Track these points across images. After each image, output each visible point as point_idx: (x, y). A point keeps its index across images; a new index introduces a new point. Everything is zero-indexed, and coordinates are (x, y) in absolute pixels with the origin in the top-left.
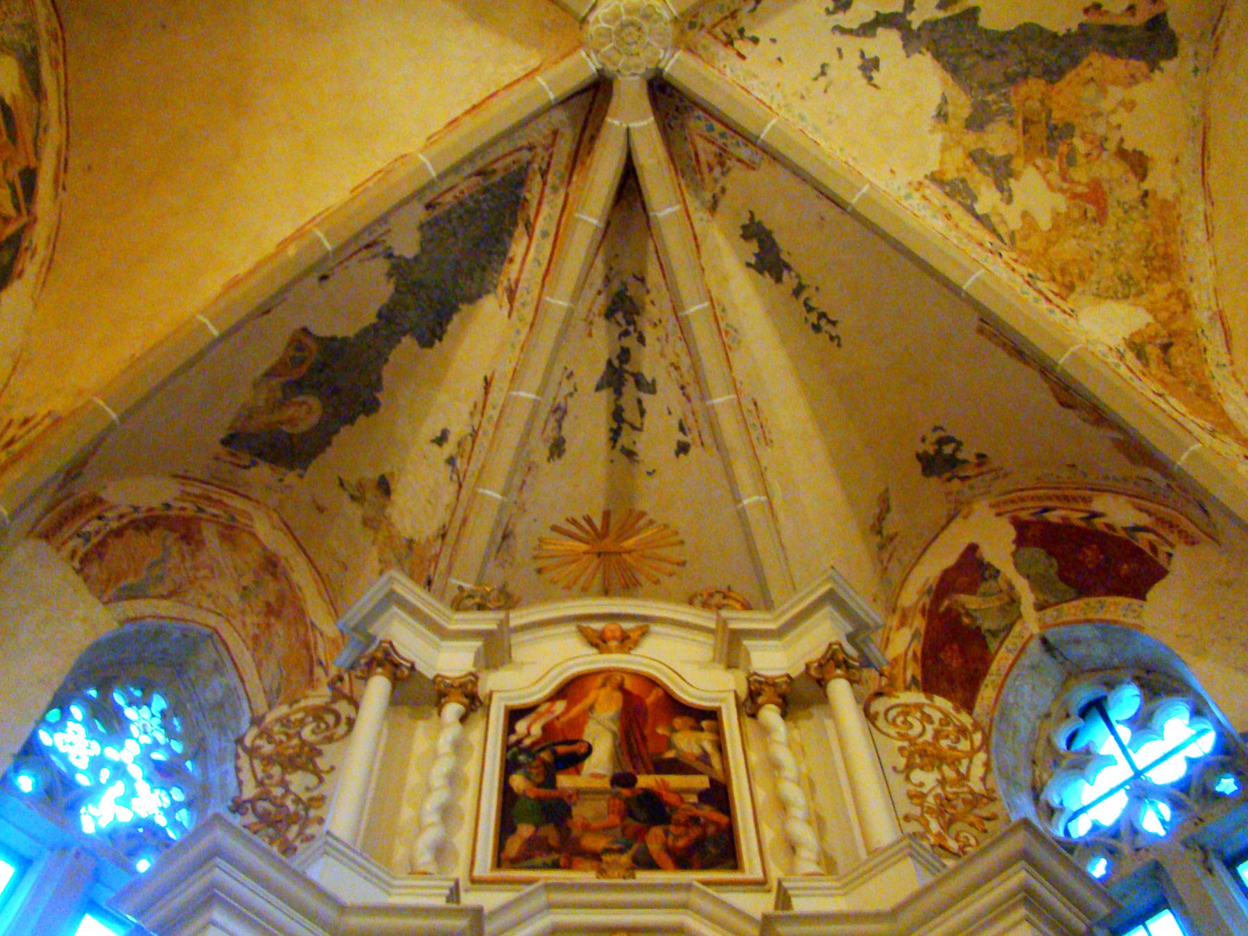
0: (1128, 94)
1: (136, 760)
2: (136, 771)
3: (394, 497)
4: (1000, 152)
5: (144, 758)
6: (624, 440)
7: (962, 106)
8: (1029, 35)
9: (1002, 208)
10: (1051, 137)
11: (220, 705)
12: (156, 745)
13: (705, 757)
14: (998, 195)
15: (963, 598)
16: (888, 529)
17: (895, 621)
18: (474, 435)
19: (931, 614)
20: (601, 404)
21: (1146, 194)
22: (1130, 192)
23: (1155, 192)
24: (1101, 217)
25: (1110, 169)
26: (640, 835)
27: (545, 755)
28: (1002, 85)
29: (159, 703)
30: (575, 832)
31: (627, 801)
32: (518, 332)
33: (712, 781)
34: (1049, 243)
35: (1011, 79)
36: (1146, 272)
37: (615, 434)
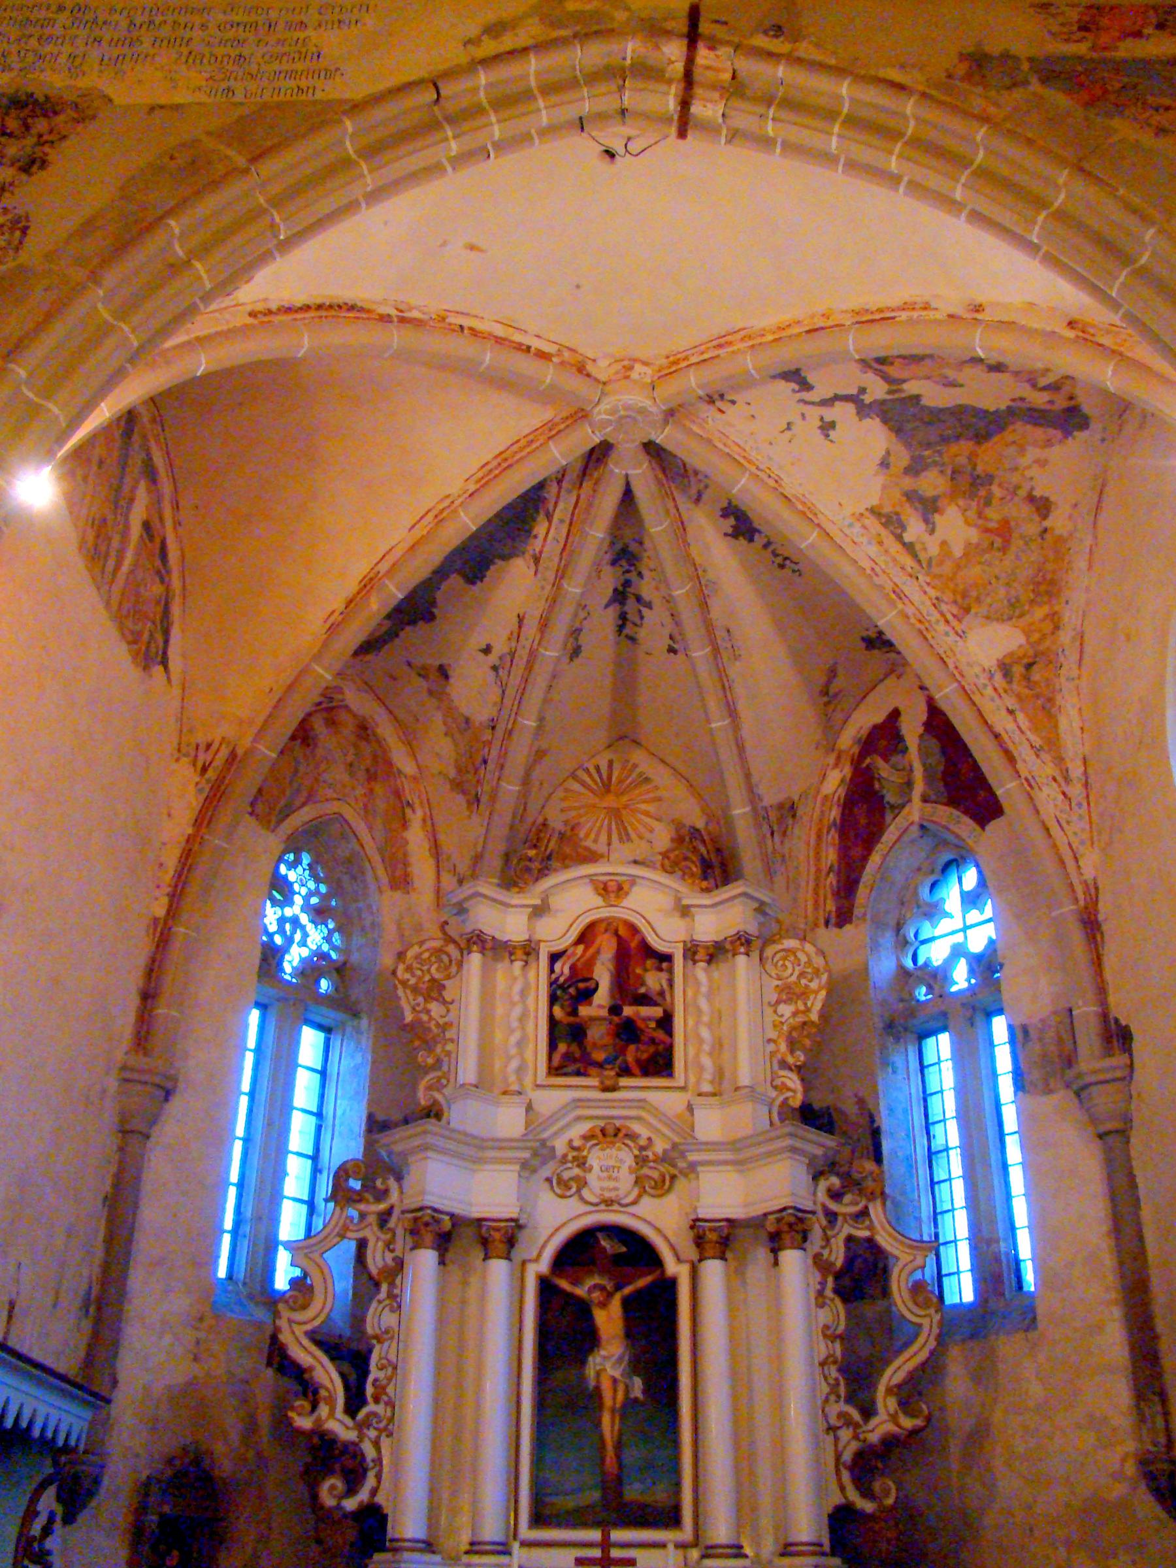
0: (1047, 453)
1: (302, 910)
2: (304, 919)
3: (452, 681)
4: (930, 493)
5: (306, 908)
6: (626, 631)
7: (902, 458)
8: (960, 412)
9: (926, 537)
10: (973, 485)
11: (349, 861)
12: (311, 894)
13: (662, 993)
14: (923, 526)
15: (880, 762)
16: (833, 689)
17: (831, 759)
18: (513, 654)
19: (857, 762)
20: (611, 614)
21: (1046, 530)
22: (1032, 528)
23: (1053, 529)
24: (1004, 549)
25: (1020, 511)
26: (623, 1051)
27: (572, 990)
28: (937, 443)
29: (306, 859)
30: (589, 1049)
31: (617, 1025)
32: (543, 588)
33: (665, 1011)
34: (959, 567)
35: (945, 440)
36: (1032, 596)
37: (621, 628)
